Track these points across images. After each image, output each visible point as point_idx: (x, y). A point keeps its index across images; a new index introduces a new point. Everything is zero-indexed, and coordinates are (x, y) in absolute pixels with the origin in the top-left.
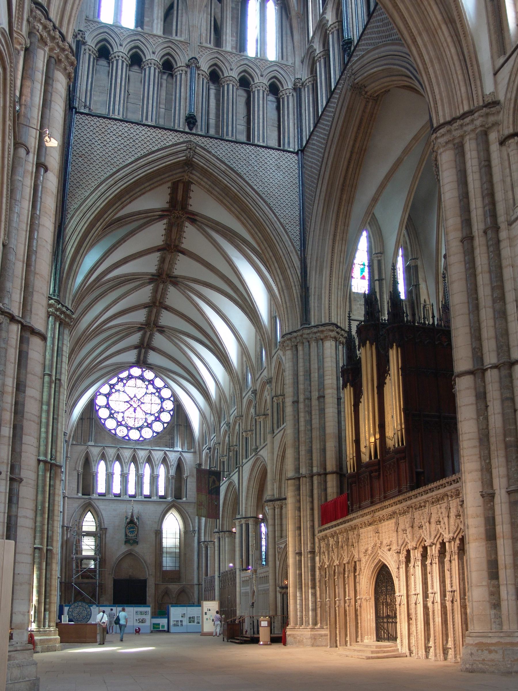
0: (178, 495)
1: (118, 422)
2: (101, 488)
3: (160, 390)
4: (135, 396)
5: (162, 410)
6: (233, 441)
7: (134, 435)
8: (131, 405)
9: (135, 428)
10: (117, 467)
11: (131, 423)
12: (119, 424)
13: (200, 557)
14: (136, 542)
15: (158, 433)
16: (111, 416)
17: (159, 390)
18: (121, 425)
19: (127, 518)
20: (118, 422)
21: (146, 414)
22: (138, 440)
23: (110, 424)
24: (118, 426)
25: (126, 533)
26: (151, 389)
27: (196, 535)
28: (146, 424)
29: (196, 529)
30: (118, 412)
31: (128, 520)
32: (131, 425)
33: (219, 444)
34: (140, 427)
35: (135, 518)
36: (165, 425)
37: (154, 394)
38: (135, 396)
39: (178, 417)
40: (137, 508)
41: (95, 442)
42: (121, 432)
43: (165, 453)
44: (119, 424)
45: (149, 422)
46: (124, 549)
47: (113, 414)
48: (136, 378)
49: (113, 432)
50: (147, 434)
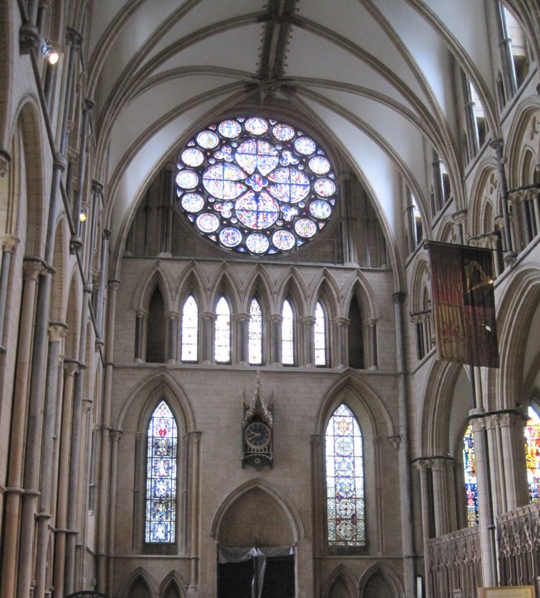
0: (356, 358)
1: (222, 219)
2: (189, 351)
3: (308, 160)
4: (257, 171)
5: (313, 197)
6: (514, 180)
7: (257, 245)
8: (249, 188)
9: (258, 232)
10: (223, 308)
11: (249, 222)
12: (225, 223)
13: (416, 496)
14: (267, 463)
15: (305, 240)
16: (209, 208)
17: (304, 160)
18: (229, 225)
19: (246, 408)
20: (222, 219)
22: (266, 253)
23: (207, 224)
25: (244, 441)
26: (289, 158)
27: (403, 445)
28: (280, 224)
29: (402, 432)
30: (223, 202)
31: (250, 413)
32: (251, 225)
33: (465, 212)
34: (268, 229)
35: (264, 407)
36: (321, 225)
37: (296, 166)
38: (257, 171)
39: (347, 204)
40: (269, 387)
41: (174, 252)
42: (230, 239)
43: (325, 273)
44: (225, 223)
45: (288, 218)
46: (241, 477)
48: (258, 138)
49: (213, 238)
50: (285, 242)
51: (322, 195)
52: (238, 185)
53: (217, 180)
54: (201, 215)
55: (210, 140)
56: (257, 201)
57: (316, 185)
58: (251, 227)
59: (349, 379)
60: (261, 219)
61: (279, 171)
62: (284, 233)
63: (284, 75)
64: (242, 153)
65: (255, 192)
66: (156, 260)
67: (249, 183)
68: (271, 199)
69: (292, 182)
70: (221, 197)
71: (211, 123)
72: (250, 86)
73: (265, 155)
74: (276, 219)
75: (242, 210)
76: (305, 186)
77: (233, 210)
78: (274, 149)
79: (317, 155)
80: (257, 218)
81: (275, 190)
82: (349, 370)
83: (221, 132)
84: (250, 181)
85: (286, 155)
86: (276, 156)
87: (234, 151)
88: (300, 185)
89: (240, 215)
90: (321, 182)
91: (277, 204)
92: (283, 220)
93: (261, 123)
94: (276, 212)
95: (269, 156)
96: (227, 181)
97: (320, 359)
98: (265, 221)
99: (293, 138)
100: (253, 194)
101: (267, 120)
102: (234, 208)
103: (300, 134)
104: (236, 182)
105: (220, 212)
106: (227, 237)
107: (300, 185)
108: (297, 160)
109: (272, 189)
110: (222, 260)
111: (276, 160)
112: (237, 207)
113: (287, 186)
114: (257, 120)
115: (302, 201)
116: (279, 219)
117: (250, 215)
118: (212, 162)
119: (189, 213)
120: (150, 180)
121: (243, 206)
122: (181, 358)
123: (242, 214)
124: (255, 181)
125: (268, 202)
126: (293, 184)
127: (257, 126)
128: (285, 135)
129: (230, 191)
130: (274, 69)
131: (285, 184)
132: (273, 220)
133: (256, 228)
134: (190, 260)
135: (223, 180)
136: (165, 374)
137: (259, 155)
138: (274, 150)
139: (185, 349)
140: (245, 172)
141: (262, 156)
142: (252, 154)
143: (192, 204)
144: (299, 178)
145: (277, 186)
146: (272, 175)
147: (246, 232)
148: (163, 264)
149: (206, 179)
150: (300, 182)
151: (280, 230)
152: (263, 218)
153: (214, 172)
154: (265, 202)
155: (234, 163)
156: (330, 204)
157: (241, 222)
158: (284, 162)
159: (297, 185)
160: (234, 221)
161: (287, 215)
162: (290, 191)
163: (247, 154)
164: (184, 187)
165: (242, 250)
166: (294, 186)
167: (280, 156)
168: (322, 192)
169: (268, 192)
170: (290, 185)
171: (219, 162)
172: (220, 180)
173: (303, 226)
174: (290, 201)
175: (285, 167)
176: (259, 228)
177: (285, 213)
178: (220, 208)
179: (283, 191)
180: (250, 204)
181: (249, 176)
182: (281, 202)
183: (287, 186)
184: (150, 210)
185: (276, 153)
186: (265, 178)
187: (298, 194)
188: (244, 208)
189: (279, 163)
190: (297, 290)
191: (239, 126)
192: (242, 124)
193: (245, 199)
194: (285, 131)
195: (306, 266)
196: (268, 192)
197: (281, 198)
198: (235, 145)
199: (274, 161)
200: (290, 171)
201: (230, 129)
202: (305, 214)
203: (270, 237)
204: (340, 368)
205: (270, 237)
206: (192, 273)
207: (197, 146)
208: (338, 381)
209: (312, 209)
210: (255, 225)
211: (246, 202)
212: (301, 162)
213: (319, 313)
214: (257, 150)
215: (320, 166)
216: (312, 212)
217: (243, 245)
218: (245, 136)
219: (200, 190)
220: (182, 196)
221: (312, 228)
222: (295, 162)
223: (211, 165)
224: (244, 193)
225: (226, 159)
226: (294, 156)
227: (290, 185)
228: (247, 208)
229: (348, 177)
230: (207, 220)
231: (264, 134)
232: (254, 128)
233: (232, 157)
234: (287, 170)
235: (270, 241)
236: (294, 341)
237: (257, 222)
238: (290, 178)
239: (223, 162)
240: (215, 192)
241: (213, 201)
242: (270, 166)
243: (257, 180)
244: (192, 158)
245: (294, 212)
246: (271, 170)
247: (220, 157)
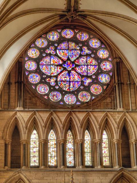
0: (126, 162)
2: (34, 161)
4: (68, 59)
5: (100, 71)
8: (65, 69)
10: (52, 136)
12: (52, 89)
18: (55, 90)
20: (50, 86)
21: (83, 76)
23: (42, 90)
24: (51, 91)
26: (87, 51)
28: (82, 87)
30: (50, 77)
34: (76, 91)
38: (68, 59)
39: (119, 75)
44: (52, 89)
45: (86, 84)
47: (45, 79)
48: (69, 40)
51: (105, 70)
52: (59, 67)
53: (47, 65)
54: (39, 85)
55: (43, 42)
56: (69, 76)
57: (102, 65)
58: (66, 90)
59: (123, 173)
60: (72, 86)
61: (81, 58)
62: (84, 93)
63: (80, 9)
64: (61, 49)
65: (68, 70)
66: (14, 112)
67: (65, 66)
68: (77, 74)
69: (88, 64)
70: (49, 75)
71: (43, 34)
72: (61, 16)
73: (73, 50)
74: (80, 85)
75: (61, 81)
76: (95, 66)
77: (56, 81)
78: (78, 46)
79: (102, 48)
80: (70, 85)
81: (79, 69)
82: (122, 168)
83: (48, 38)
84: (65, 65)
85: (84, 49)
86: (79, 50)
87: (56, 48)
88: (93, 65)
89: (60, 84)
90: (104, 63)
91: (80, 77)
92: (84, 86)
93: (70, 32)
94: (80, 81)
95: (75, 50)
96: (52, 65)
97: (106, 162)
98: (74, 87)
99: (88, 39)
100: (67, 72)
101: (73, 29)
102: (57, 80)
103: (91, 37)
104: (57, 66)
105: (49, 83)
106: (53, 96)
107: (93, 65)
108: (91, 51)
109: (77, 68)
110: (51, 110)
111: (79, 52)
112: (59, 79)
113: (85, 66)
114: (68, 30)
115: (94, 74)
116: (81, 85)
117: (65, 84)
118: (44, 55)
119: (33, 84)
120: (10, 69)
121: (62, 79)
122: (30, 164)
123: (61, 83)
124: (68, 65)
125: (75, 76)
126: (89, 65)
127: (69, 34)
128: (83, 38)
129: (54, 71)
130: (74, 6)
131: (84, 65)
132: (78, 86)
133: (69, 91)
134: (34, 111)
135: (51, 65)
136: (21, 175)
137: (70, 50)
138: (78, 47)
139: (32, 159)
140: (62, 60)
141: (71, 50)
142: (65, 50)
143: (35, 79)
144: (92, 61)
145: (80, 67)
146: (77, 60)
147: (64, 93)
148: (18, 114)
149: (41, 65)
150: (92, 64)
151: (82, 91)
152: (73, 85)
153: (45, 61)
154: (73, 76)
155: (56, 55)
156: (109, 75)
157: (61, 88)
158: (84, 53)
159: (91, 65)
160: (57, 87)
161: (86, 82)
162: (87, 69)
163: (63, 49)
164: (29, 69)
165: (62, 103)
166: (89, 66)
167: (81, 50)
168: (105, 69)
169: (76, 71)
170: (87, 66)
171: (48, 55)
172: (49, 65)
173: (95, 88)
174: (87, 75)
175: (84, 56)
176: (71, 91)
177: (85, 81)
178: (49, 80)
179: (84, 69)
180: (65, 77)
181: (64, 62)
182: (82, 75)
183: (85, 66)
184: (11, 84)
185: (78, 48)
186: (73, 63)
187: (91, 70)
188: (62, 80)
189: (81, 54)
190: (92, 125)
191: (58, 34)
192: (60, 33)
193: (62, 75)
194: (83, 35)
195: (97, 111)
196: (76, 71)
197: (82, 73)
198: (56, 45)
199: (78, 53)
200: (87, 58)
201: (54, 36)
202: (96, 81)
203: (77, 96)
204: (117, 167)
205: (77, 96)
206: (35, 118)
207: (36, 47)
208: (116, 175)
209: (100, 79)
210: (68, 89)
211: (64, 77)
212: (93, 53)
213: (105, 136)
214: (68, 47)
215: (103, 54)
216: (99, 80)
217: (62, 100)
218: (62, 40)
219: (38, 71)
220: (28, 75)
221: (100, 89)
222: (89, 53)
223: (44, 57)
224: (61, 72)
225: (51, 53)
226: (89, 49)
227: (87, 66)
228: (64, 80)
229: (118, 60)
230: (42, 87)
231: (72, 38)
232: (66, 35)
233: (55, 52)
234: (85, 57)
235: (77, 97)
236: (91, 152)
237: (70, 87)
238: (87, 62)
239: (50, 55)
240: (46, 71)
241: (45, 76)
242: (76, 56)
243: (69, 64)
244: (33, 53)
245: (88, 81)
246: (76, 58)
247: (49, 52)
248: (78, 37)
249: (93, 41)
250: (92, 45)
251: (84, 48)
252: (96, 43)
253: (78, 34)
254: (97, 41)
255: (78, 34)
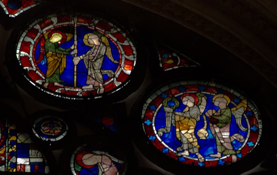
78: (21, 139)
138: (23, 152)
194: (84, 49)
248: (25, 59)
249: (189, 103)
250: (176, 143)
251: (89, 160)
252: (213, 121)
253: (24, 38)
254: (221, 102)
255: (32, 33)
